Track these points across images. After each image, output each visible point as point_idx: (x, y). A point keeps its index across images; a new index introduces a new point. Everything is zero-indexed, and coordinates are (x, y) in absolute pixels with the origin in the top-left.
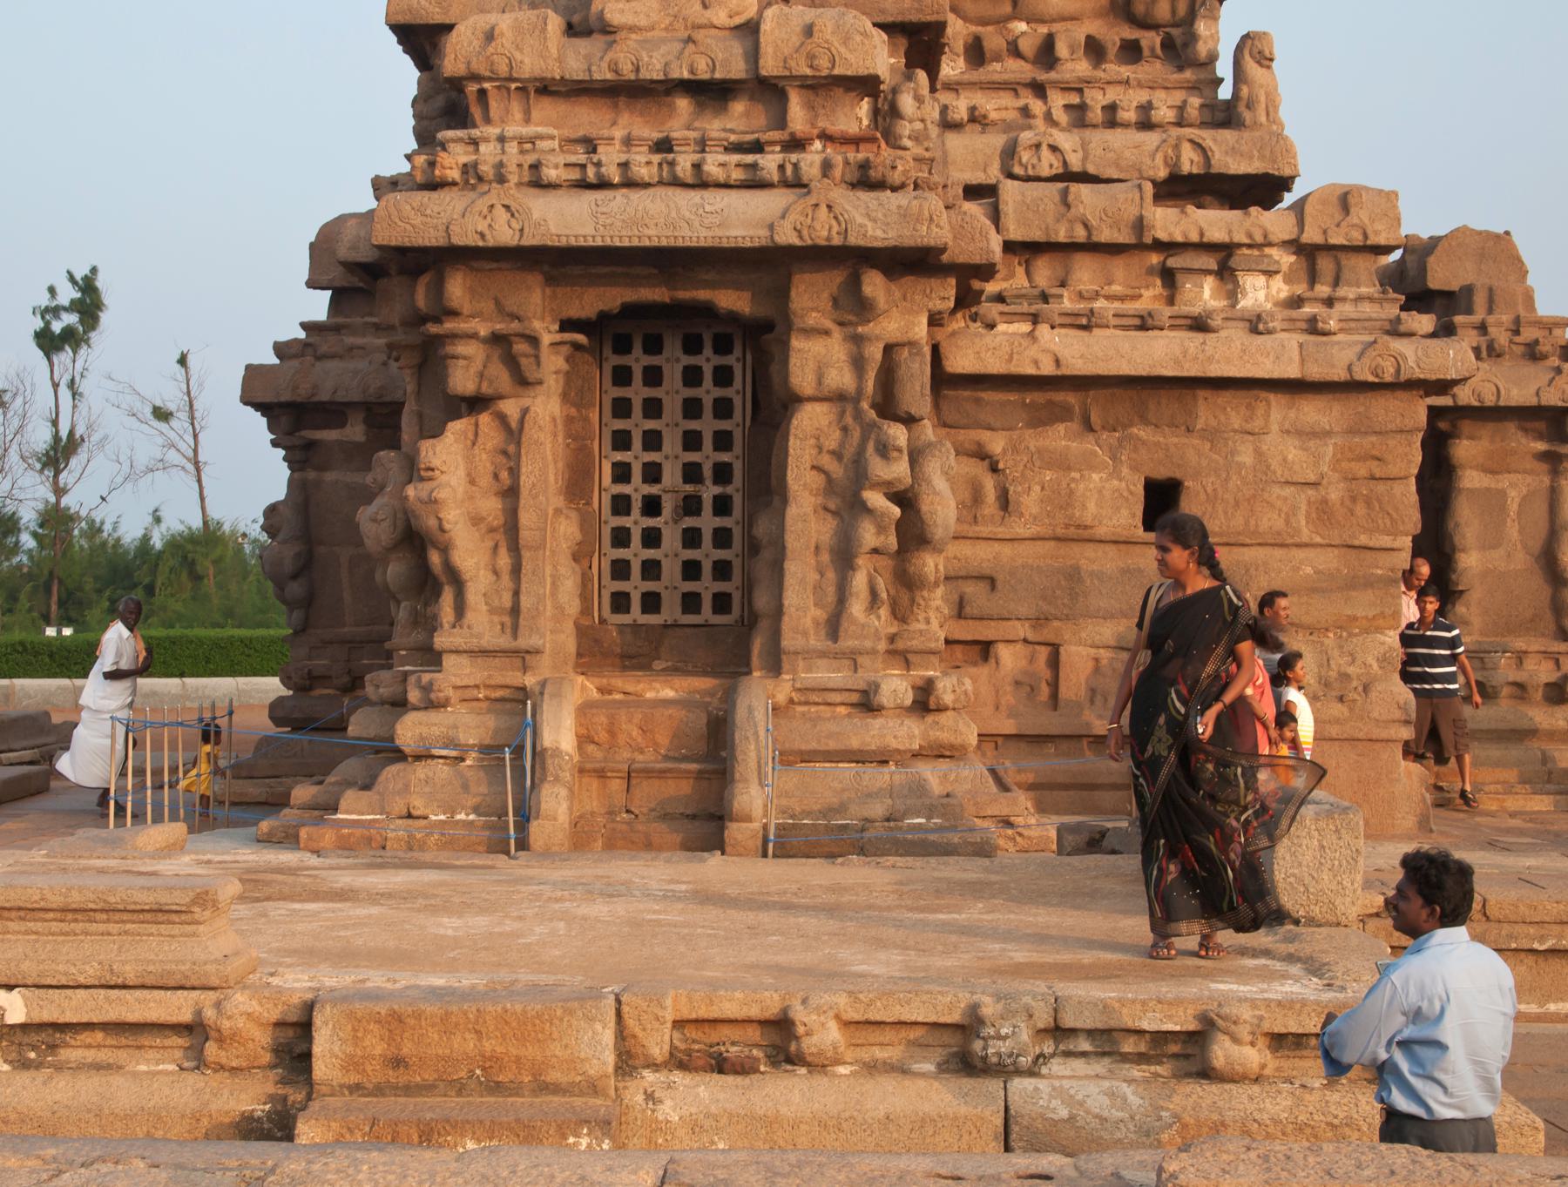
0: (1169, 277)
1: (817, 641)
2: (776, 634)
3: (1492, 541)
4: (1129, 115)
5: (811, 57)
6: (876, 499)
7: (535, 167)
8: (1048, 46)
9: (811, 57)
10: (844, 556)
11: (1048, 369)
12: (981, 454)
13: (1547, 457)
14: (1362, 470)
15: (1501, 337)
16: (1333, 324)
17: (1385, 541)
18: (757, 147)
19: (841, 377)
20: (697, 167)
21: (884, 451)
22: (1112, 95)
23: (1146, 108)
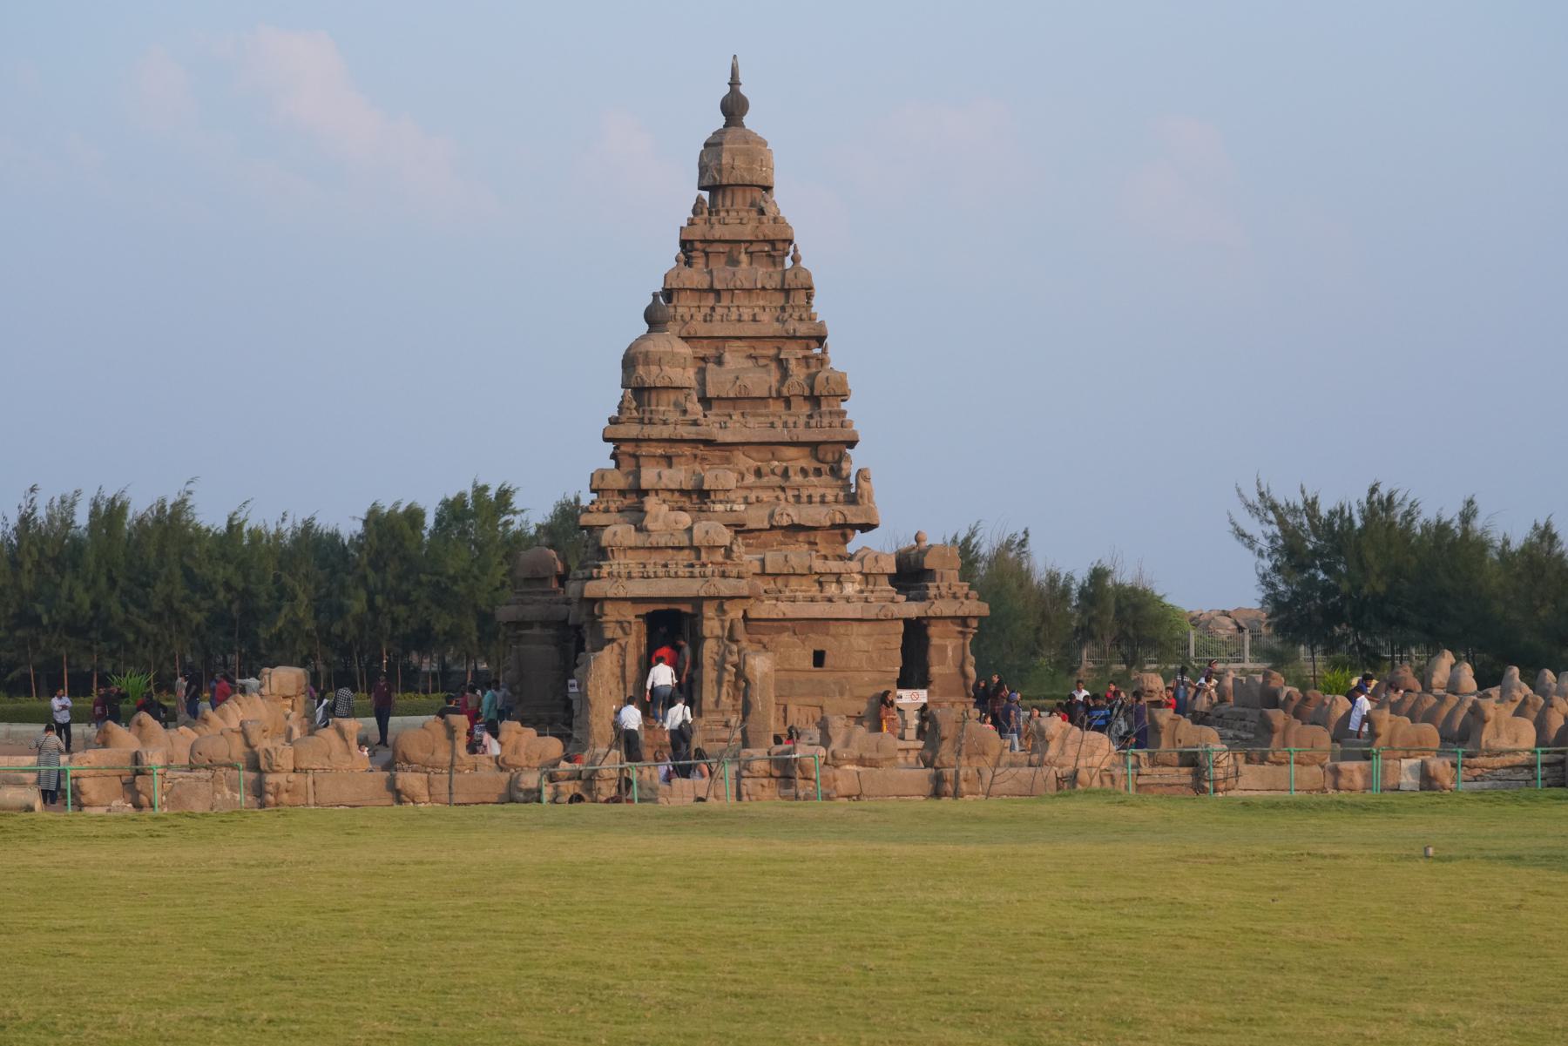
0: (820, 584)
1: (712, 707)
2: (700, 706)
3: (942, 662)
4: (817, 499)
5: (708, 541)
6: (728, 667)
7: (629, 573)
8: (786, 470)
9: (708, 541)
10: (720, 682)
11: (781, 616)
12: (760, 642)
13: (961, 632)
14: (883, 646)
15: (944, 591)
16: (873, 599)
17: (889, 669)
18: (692, 566)
19: (718, 632)
20: (676, 573)
21: (731, 652)
22: (811, 491)
23: (823, 496)
